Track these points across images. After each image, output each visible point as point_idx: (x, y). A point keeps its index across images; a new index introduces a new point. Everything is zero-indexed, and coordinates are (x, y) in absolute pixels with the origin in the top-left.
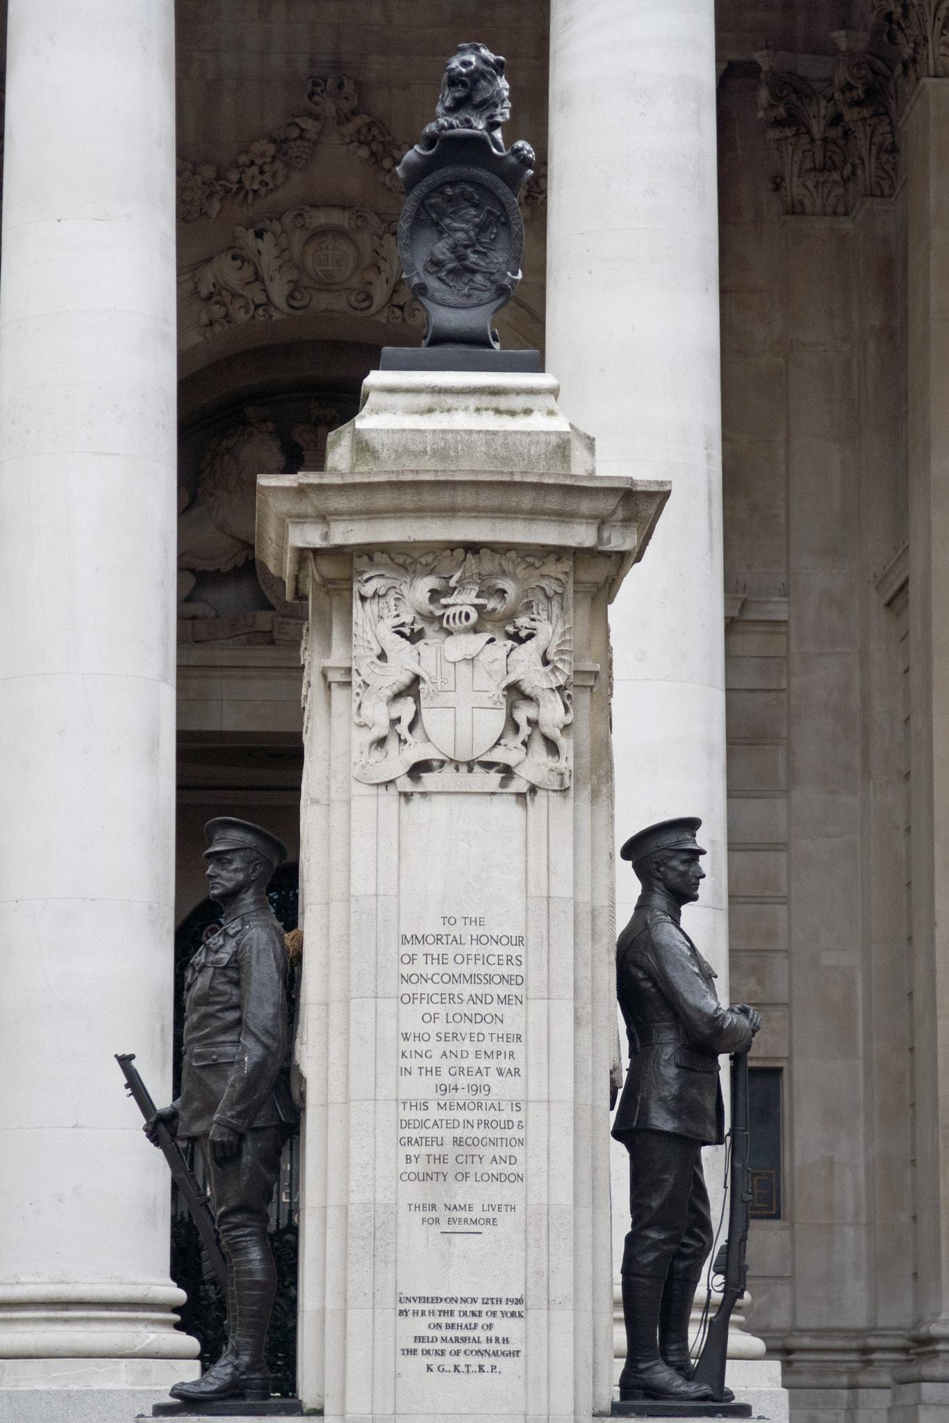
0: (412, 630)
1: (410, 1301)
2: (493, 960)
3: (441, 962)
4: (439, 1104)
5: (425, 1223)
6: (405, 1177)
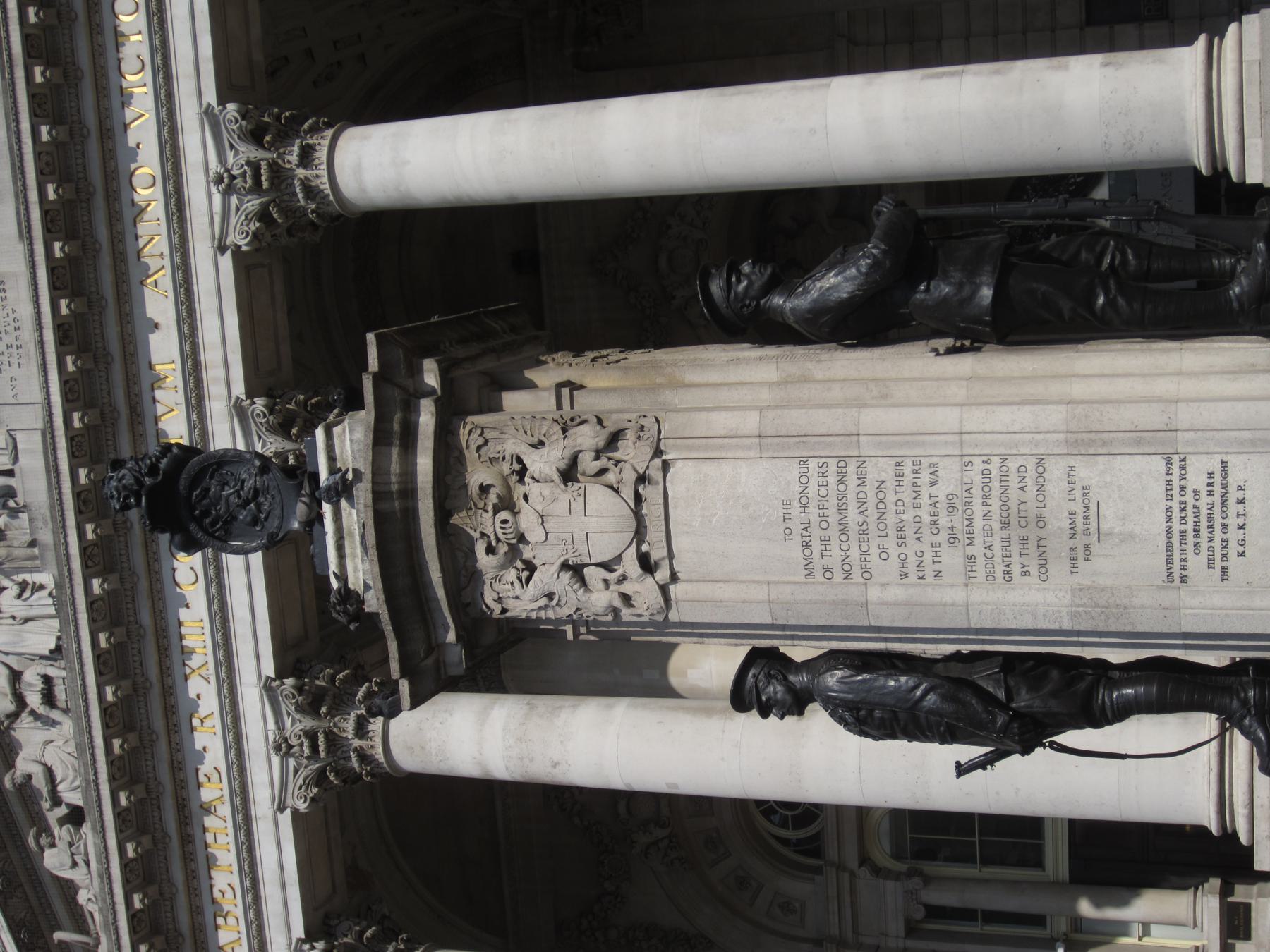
0: (523, 570)
1: (1172, 573)
2: (823, 491)
3: (828, 542)
4: (968, 545)
5: (1090, 558)
6: (1043, 577)
